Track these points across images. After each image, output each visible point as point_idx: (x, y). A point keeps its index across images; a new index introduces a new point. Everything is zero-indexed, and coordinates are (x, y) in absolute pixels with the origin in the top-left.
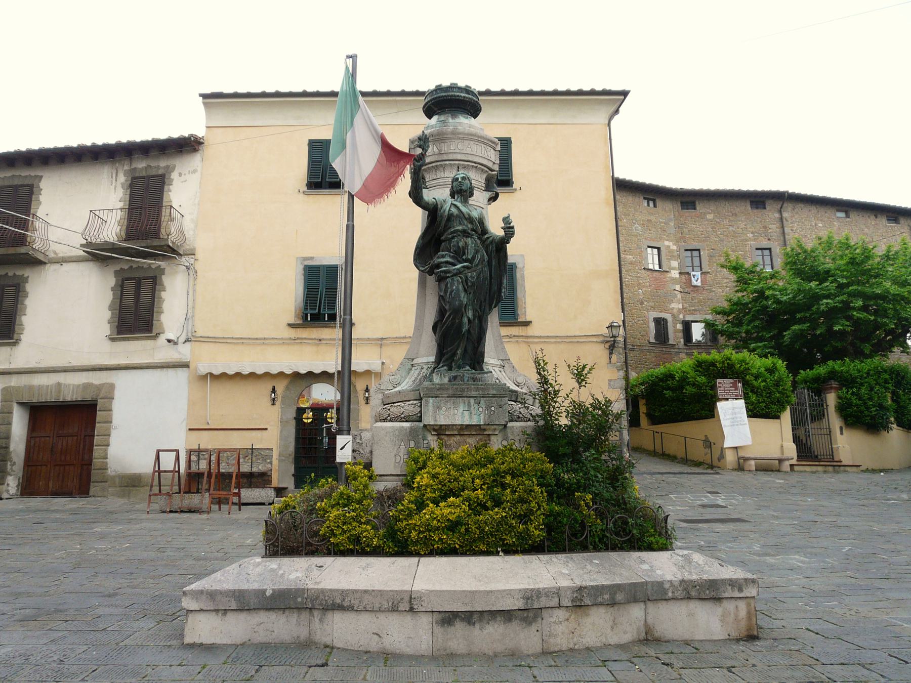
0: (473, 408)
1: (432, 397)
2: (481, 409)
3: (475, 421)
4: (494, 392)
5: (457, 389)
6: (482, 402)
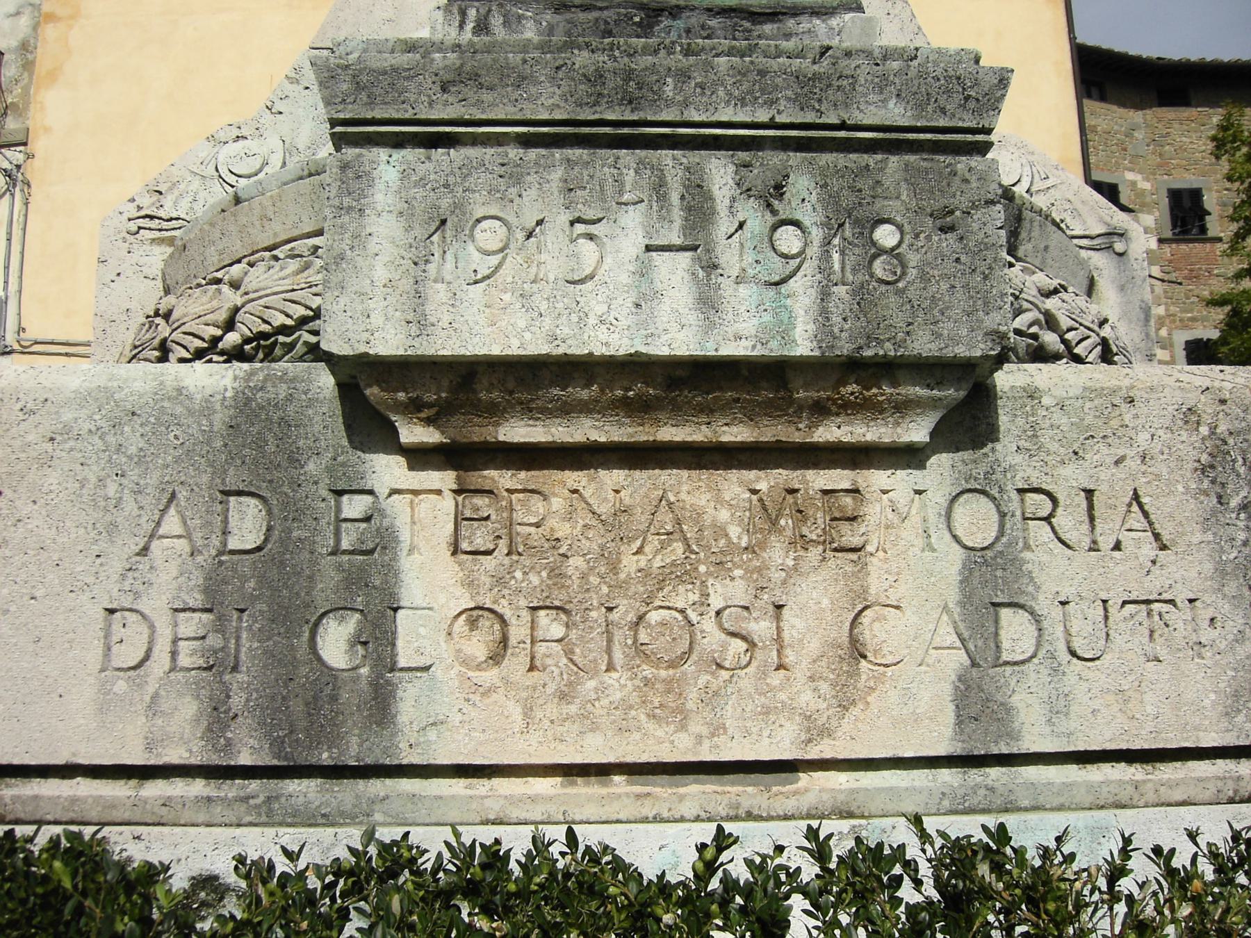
0: (724, 225)
1: (398, 142)
2: (789, 240)
3: (748, 326)
4: (896, 113)
5: (596, 78)
6: (802, 185)
